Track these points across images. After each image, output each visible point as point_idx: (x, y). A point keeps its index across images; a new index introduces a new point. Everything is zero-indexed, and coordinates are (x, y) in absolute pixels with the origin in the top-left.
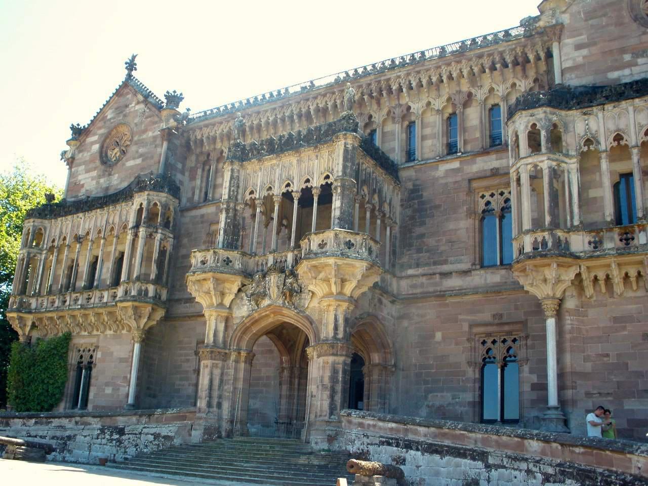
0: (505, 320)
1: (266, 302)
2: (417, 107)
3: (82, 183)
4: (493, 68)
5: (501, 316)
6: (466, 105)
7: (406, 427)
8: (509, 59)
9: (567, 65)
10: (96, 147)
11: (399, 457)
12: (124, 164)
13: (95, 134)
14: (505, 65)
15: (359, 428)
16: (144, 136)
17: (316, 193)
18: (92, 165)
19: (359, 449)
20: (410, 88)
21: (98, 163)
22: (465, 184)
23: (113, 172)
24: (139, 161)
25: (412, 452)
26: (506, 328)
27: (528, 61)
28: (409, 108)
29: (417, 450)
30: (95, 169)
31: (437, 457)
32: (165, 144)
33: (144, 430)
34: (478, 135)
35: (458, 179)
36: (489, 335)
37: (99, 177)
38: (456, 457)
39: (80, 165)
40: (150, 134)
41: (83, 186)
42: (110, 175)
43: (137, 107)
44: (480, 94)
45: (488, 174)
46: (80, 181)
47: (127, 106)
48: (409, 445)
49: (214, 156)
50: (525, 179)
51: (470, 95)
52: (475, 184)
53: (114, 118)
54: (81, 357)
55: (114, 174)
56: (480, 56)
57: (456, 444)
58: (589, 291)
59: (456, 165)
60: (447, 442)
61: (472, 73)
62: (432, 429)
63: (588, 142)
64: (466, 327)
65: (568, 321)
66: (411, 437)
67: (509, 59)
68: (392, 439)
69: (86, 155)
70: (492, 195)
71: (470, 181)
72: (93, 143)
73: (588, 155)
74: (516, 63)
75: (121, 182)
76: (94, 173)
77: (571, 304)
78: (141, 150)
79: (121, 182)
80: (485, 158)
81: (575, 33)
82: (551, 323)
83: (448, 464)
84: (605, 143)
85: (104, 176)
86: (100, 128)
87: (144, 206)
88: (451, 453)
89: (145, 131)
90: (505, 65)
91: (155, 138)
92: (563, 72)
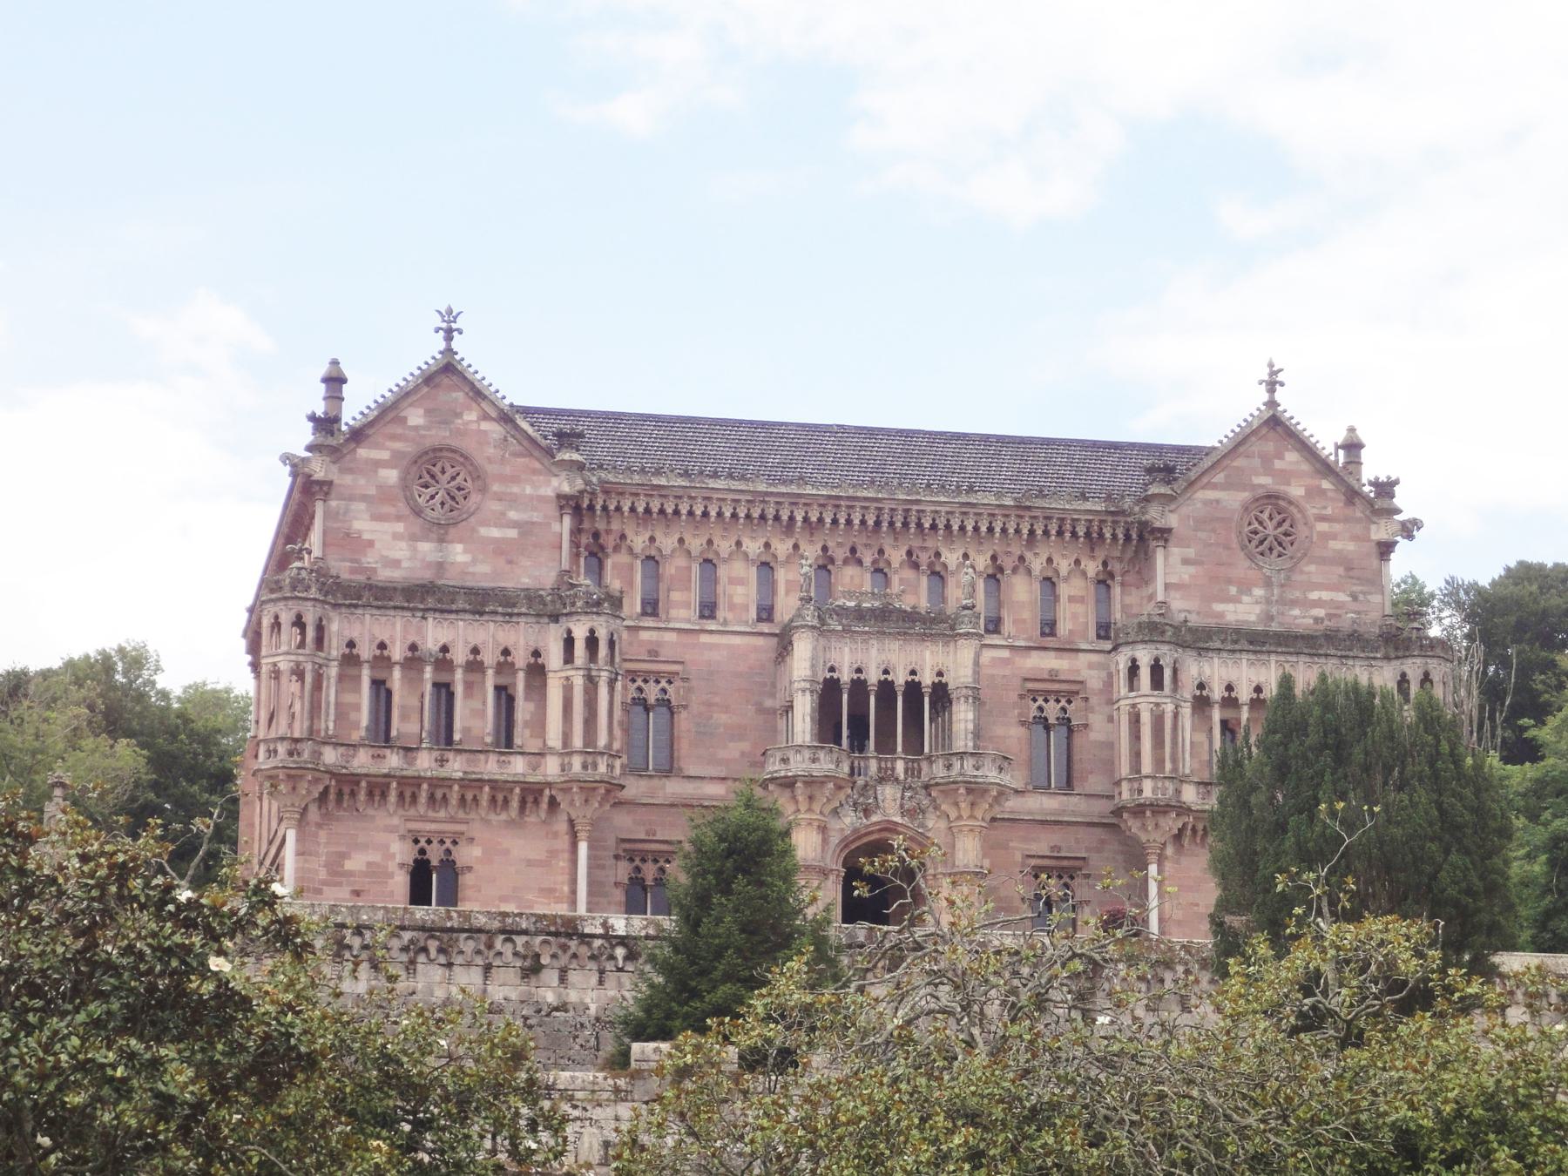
0: (1063, 854)
1: (874, 818)
2: (951, 558)
3: (366, 536)
4: (1060, 533)
5: (1060, 849)
6: (1015, 570)
8: (1081, 531)
9: (1173, 580)
10: (391, 476)
12: (473, 530)
13: (378, 446)
14: (1074, 534)
16: (515, 489)
17: (927, 691)
18: (387, 509)
20: (948, 527)
21: (403, 508)
22: (1017, 682)
23: (449, 537)
24: (512, 533)
26: (1065, 863)
27: (1101, 535)
28: (938, 555)
30: (399, 518)
32: (567, 520)
34: (1026, 615)
35: (1007, 672)
36: (1042, 869)
37: (414, 538)
39: (351, 498)
40: (528, 490)
41: (371, 543)
42: (441, 540)
43: (485, 426)
44: (1037, 564)
45: (1046, 676)
46: (360, 532)
47: (459, 415)
49: (609, 541)
50: (1146, 718)
51: (1022, 558)
52: (1030, 685)
53: (423, 428)
54: (422, 852)
55: (452, 542)
56: (1048, 518)
58: (1186, 842)
59: (1005, 654)
61: (1032, 532)
63: (1201, 686)
64: (1018, 857)
65: (1168, 866)
67: (1081, 531)
69: (362, 484)
70: (1046, 701)
71: (1026, 680)
72: (378, 464)
73: (1202, 703)
74: (1088, 534)
75: (474, 561)
76: (400, 527)
77: (1169, 851)
78: (513, 515)
79: (474, 561)
80: (1042, 653)
81: (1183, 543)
82: (1153, 869)
84: (1217, 693)
85: (426, 539)
86: (394, 437)
87: (602, 634)
89: (514, 479)
90: (1074, 534)
91: (542, 499)
92: (1167, 586)
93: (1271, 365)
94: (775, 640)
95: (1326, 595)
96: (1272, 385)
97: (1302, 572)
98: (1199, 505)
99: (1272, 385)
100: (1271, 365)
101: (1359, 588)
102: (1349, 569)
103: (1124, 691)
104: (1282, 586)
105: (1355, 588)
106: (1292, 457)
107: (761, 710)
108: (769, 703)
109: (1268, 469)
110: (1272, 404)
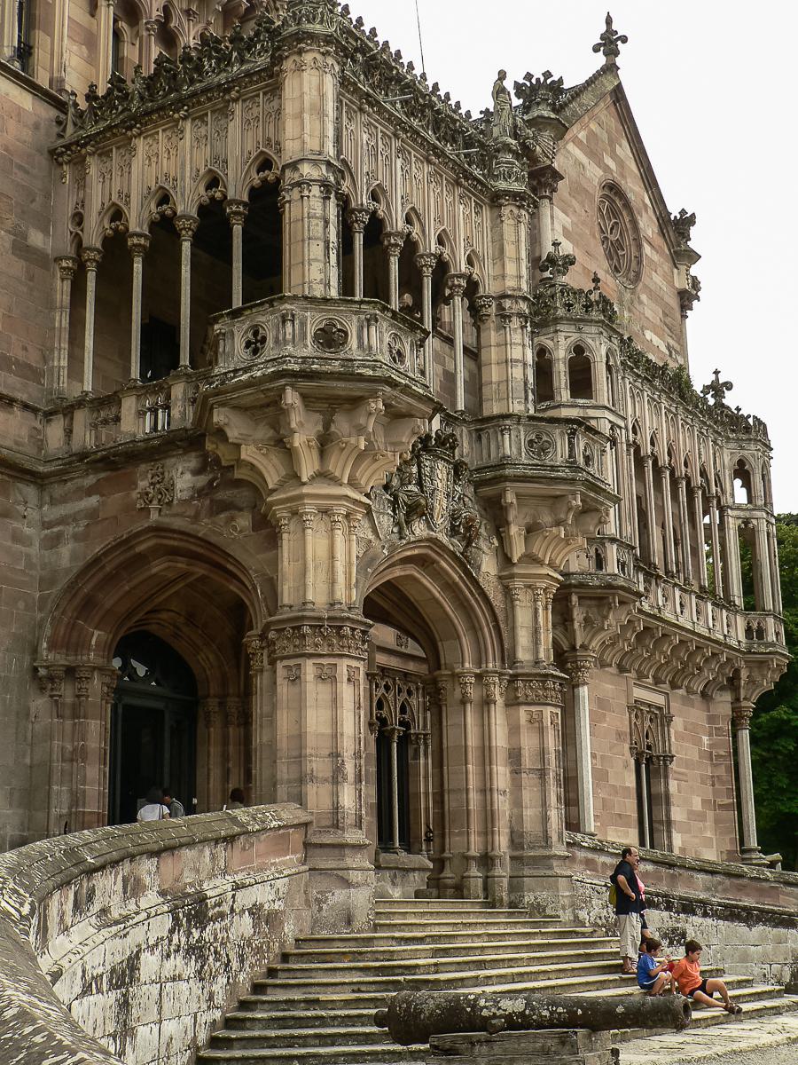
7: (671, 871)
11: (674, 930)
15: (588, 872)
19: (600, 918)
25: (697, 920)
29: (705, 915)
31: (741, 928)
33: (239, 894)
38: (775, 926)
48: (688, 907)
57: (764, 904)
60: (748, 902)
62: (719, 878)
66: (681, 891)
68: (657, 895)
83: (764, 939)
88: (766, 920)
93: (609, 21)
94: (48, 113)
95: (656, 341)
96: (610, 43)
97: (641, 302)
98: (571, 162)
99: (610, 43)
100: (609, 21)
101: (672, 342)
102: (665, 315)
103: (565, 395)
104: (630, 311)
105: (672, 342)
106: (624, 150)
107: (22, 249)
108: (36, 239)
109: (614, 156)
110: (611, 69)
